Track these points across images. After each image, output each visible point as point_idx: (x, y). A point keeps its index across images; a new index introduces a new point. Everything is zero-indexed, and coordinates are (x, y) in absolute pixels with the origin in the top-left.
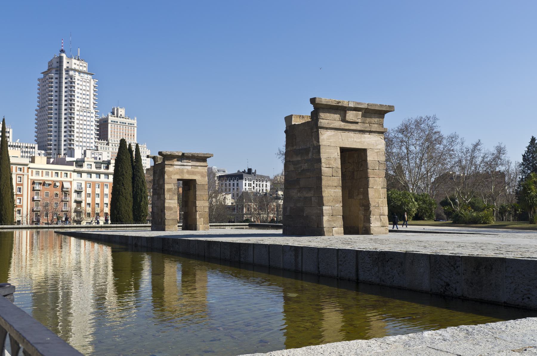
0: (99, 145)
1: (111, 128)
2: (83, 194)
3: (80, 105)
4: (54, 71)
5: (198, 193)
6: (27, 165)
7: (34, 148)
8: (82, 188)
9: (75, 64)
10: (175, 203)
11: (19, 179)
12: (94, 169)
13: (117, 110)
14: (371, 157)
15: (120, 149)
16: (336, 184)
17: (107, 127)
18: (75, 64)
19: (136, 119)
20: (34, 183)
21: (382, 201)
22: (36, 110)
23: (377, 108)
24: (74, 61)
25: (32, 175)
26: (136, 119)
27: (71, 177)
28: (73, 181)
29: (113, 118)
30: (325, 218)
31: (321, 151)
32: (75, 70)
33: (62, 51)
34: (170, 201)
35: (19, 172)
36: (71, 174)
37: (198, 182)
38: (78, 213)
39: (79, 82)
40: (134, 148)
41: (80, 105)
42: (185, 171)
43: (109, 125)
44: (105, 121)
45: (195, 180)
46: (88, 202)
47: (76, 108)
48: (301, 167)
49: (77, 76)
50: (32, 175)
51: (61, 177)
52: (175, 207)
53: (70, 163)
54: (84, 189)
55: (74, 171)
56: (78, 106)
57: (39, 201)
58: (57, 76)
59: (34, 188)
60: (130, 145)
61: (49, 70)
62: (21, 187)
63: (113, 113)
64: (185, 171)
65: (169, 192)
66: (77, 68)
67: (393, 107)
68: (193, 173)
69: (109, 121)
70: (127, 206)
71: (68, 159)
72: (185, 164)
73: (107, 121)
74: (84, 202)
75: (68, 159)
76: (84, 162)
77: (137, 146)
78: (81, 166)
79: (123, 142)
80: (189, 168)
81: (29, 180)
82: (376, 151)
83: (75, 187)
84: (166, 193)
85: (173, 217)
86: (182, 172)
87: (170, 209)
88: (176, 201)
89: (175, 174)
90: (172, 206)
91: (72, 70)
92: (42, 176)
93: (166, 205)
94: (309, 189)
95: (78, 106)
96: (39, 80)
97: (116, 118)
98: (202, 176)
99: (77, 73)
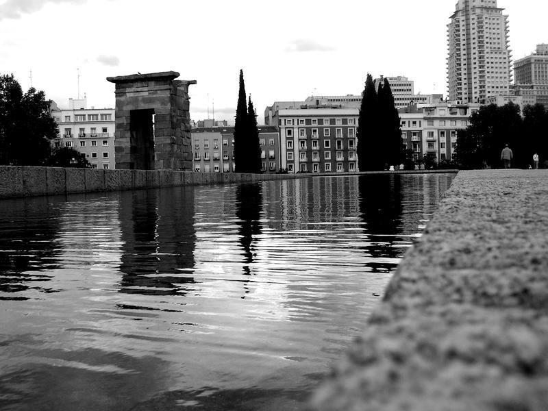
1: (535, 68)
10: (127, 142)
12: (448, 115)
27: (420, 126)
34: (121, 140)
36: (420, 122)
39: (487, 21)
42: (140, 98)
43: (533, 66)
46: (441, 152)
52: (126, 147)
53: (420, 111)
55: (425, 119)
64: (140, 98)
65: (120, 128)
68: (150, 101)
69: (533, 61)
72: (139, 89)
80: (146, 94)
86: (135, 100)
88: (129, 140)
89: (127, 104)
90: (123, 146)
92: (409, 126)
96: (447, 26)
97: (540, 56)
98: (163, 103)
99: (484, 11)
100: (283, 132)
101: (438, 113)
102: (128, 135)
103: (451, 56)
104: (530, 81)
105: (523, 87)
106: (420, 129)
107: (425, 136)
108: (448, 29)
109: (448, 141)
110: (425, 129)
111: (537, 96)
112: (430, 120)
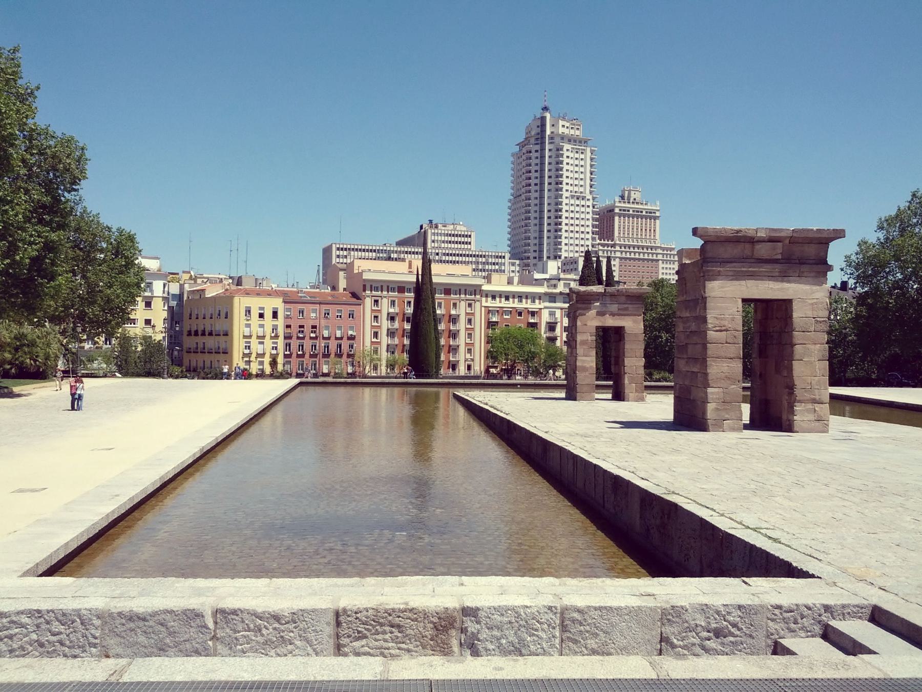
0: (601, 248)
3: (570, 188)
4: (533, 141)
5: (627, 346)
6: (481, 286)
7: (504, 257)
8: (556, 319)
9: (563, 126)
13: (630, 191)
14: (798, 314)
16: (732, 356)
17: (613, 220)
18: (563, 126)
19: (658, 203)
21: (819, 381)
22: (510, 201)
23: (811, 235)
24: (561, 123)
26: (658, 203)
29: (623, 205)
30: (710, 407)
31: (708, 305)
32: (563, 138)
33: (545, 109)
34: (584, 358)
37: (627, 330)
39: (569, 154)
41: (570, 188)
43: (617, 218)
44: (610, 211)
45: (624, 327)
47: (565, 194)
48: (689, 327)
49: (567, 146)
52: (591, 367)
53: (539, 282)
54: (559, 320)
55: (546, 294)
56: (567, 190)
58: (538, 147)
61: (526, 139)
63: (622, 197)
66: (566, 131)
67: (844, 231)
69: (617, 210)
71: (537, 276)
73: (612, 211)
75: (537, 276)
76: (559, 280)
78: (555, 286)
82: (810, 302)
83: (545, 317)
84: (578, 346)
85: (588, 381)
87: (584, 369)
88: (594, 359)
91: (558, 135)
93: (578, 364)
94: (696, 360)
95: (567, 190)
96: (513, 155)
100: (368, 302)
102: (594, 353)
103: (517, 196)
104: (611, 236)
105: (603, 245)
107: (545, 317)
108: (512, 159)
110: (546, 308)
111: (621, 258)
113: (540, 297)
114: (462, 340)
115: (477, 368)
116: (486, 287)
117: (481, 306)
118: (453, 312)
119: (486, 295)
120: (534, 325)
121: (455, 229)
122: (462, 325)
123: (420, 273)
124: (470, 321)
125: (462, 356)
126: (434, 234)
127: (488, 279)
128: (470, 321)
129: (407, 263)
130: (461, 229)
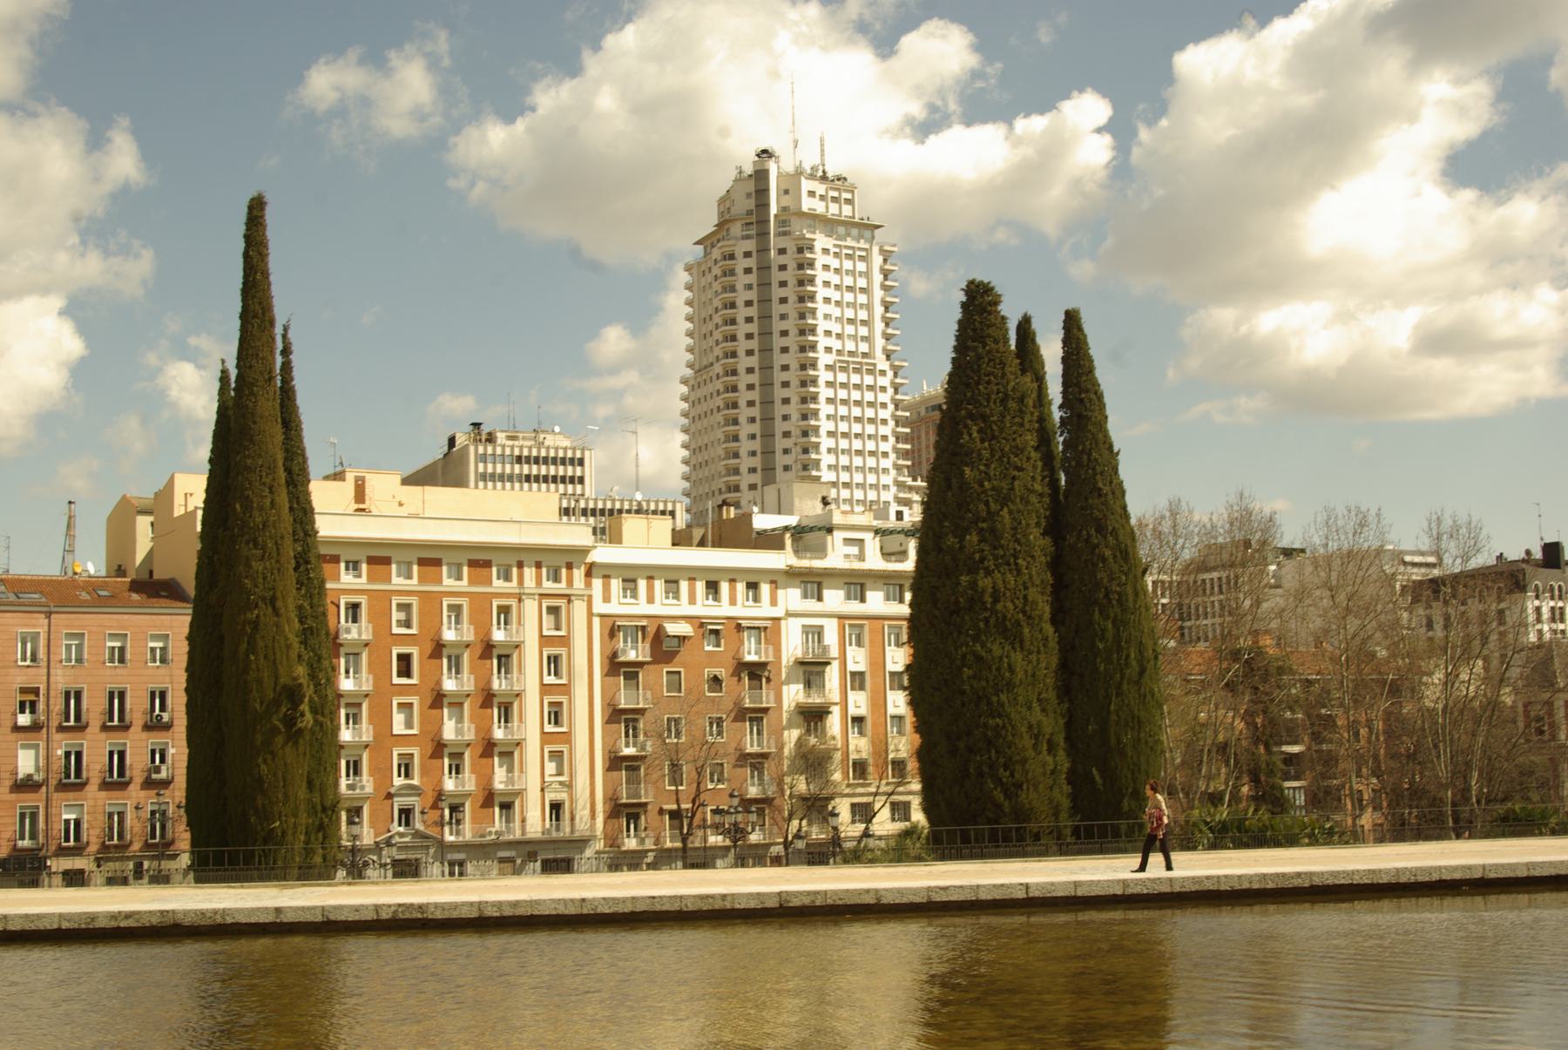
2: (832, 675)
6: (584, 551)
11: (548, 620)
15: (961, 347)
20: (612, 632)
25: (607, 598)
28: (794, 621)
35: (548, 586)
38: (813, 762)
40: (1051, 351)
50: (607, 598)
51: (733, 602)
57: (641, 712)
59: (615, 655)
60: (1025, 327)
62: (562, 651)
70: (1033, 714)
74: (836, 710)
77: (1072, 322)
79: (979, 302)
81: (596, 621)
101: (837, 556)
106: (778, 612)
109: (878, 660)
112: (814, 583)
113: (780, 579)
114: (530, 724)
115: (583, 813)
116: (603, 554)
117: (590, 614)
118: (498, 635)
119: (607, 572)
120: (756, 672)
121: (540, 445)
122: (530, 675)
123: (233, 377)
124: (554, 660)
125: (531, 779)
126: (483, 458)
127: (608, 532)
128: (554, 660)
129: (348, 486)
130: (556, 442)
